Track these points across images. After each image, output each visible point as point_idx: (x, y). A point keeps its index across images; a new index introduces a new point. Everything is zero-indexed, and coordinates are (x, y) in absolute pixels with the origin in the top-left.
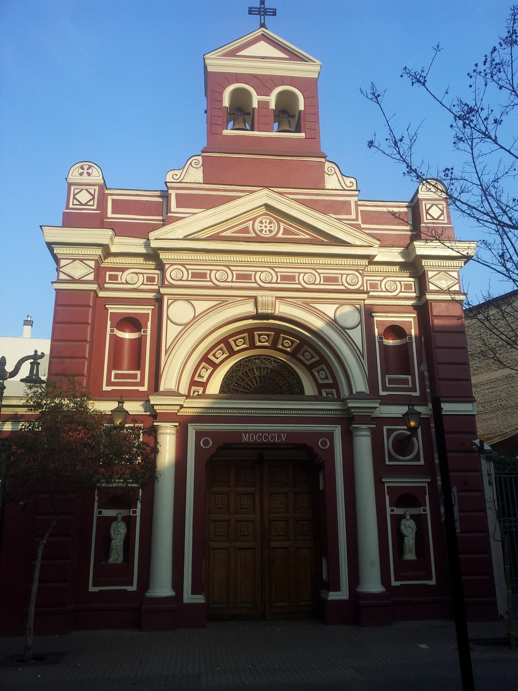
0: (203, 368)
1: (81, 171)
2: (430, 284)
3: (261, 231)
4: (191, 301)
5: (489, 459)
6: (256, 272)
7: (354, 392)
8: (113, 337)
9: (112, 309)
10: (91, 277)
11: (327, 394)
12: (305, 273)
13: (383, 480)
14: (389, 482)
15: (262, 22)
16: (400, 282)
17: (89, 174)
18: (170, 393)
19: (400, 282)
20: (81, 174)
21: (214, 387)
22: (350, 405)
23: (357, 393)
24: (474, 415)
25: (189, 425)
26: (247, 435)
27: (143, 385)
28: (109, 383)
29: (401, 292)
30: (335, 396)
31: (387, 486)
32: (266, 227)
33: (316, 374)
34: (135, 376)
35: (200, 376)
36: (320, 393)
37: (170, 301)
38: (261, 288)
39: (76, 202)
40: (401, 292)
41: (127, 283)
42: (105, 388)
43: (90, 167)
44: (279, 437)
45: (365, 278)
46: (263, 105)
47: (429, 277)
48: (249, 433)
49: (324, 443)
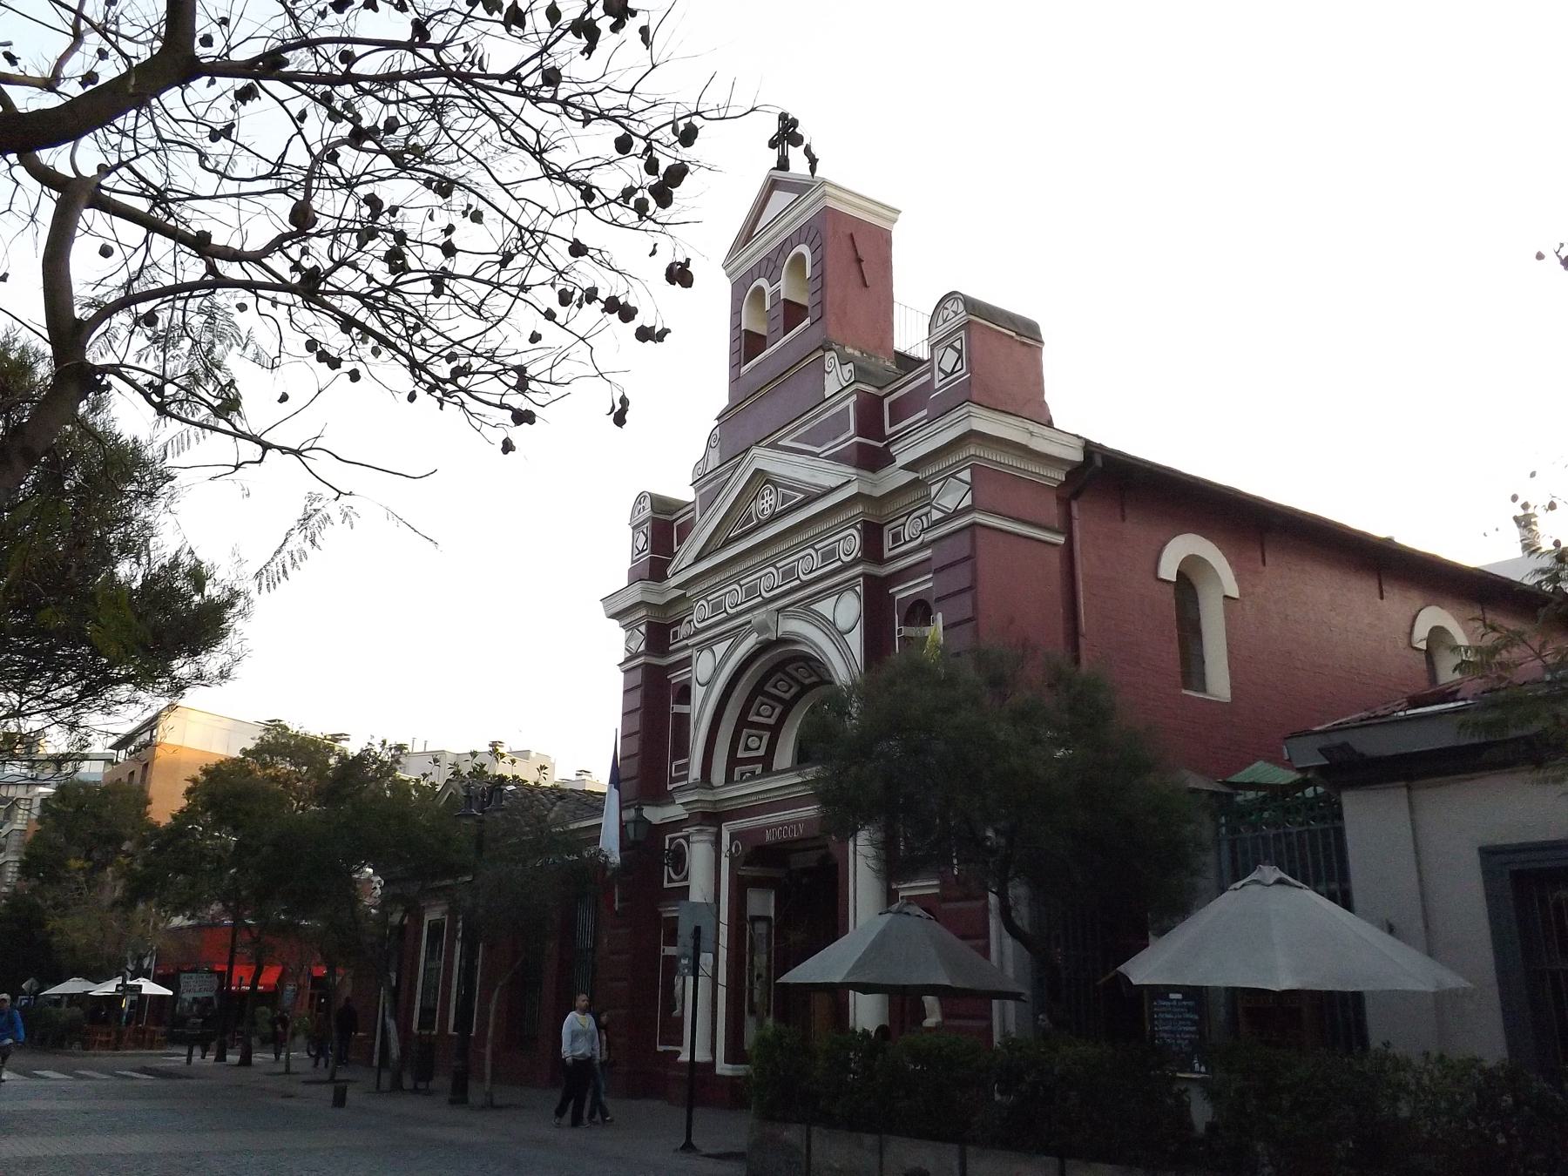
10: (642, 648)
18: (695, 787)
35: (747, 748)
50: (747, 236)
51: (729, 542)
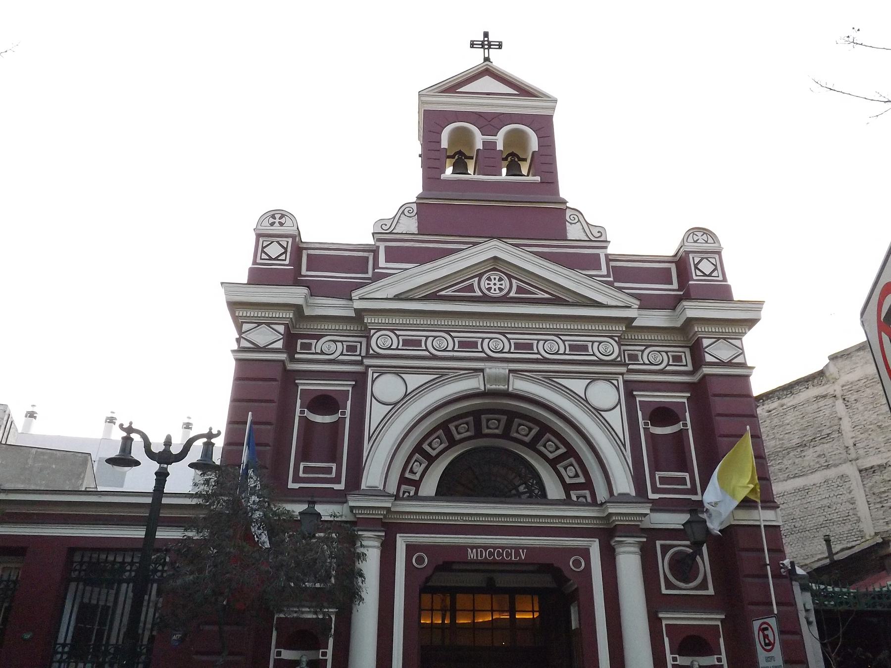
0: (416, 461)
1: (272, 220)
2: (706, 355)
3: (489, 289)
4: (403, 375)
5: (804, 588)
6: (483, 339)
7: (615, 494)
8: (305, 421)
9: (304, 385)
10: (279, 345)
11: (578, 498)
12: (546, 341)
13: (660, 615)
14: (668, 618)
15: (486, 56)
16: (666, 352)
17: (281, 224)
18: (373, 493)
19: (666, 352)
20: (272, 224)
21: (429, 487)
22: (611, 511)
23: (620, 494)
24: (779, 526)
25: (398, 535)
26: (474, 550)
27: (340, 483)
28: (296, 479)
29: (668, 365)
30: (589, 500)
31: (666, 625)
32: (495, 284)
33: (562, 470)
34: (329, 470)
35: (412, 471)
36: (568, 496)
37: (376, 375)
38: (490, 359)
39: (264, 256)
40: (668, 365)
41: (322, 353)
42: (291, 485)
43: (282, 216)
44: (517, 554)
45: (623, 348)
46: (489, 146)
47: (705, 345)
48: (477, 547)
49: (577, 563)
50: (453, 87)
51: (434, 297)
